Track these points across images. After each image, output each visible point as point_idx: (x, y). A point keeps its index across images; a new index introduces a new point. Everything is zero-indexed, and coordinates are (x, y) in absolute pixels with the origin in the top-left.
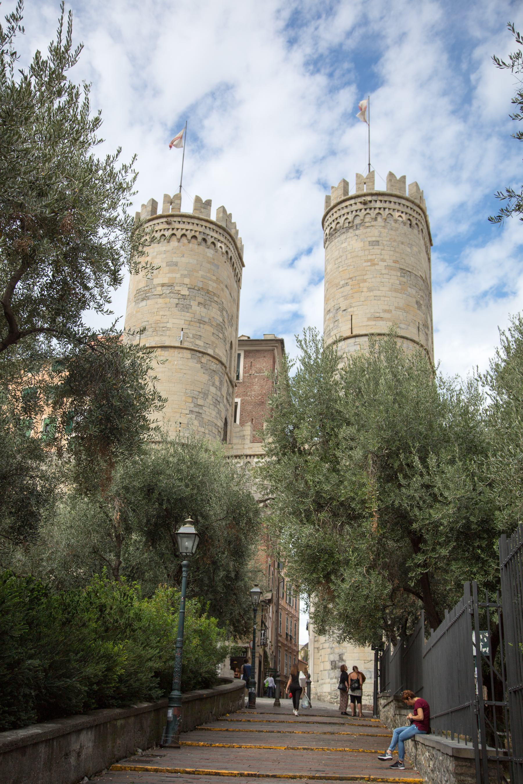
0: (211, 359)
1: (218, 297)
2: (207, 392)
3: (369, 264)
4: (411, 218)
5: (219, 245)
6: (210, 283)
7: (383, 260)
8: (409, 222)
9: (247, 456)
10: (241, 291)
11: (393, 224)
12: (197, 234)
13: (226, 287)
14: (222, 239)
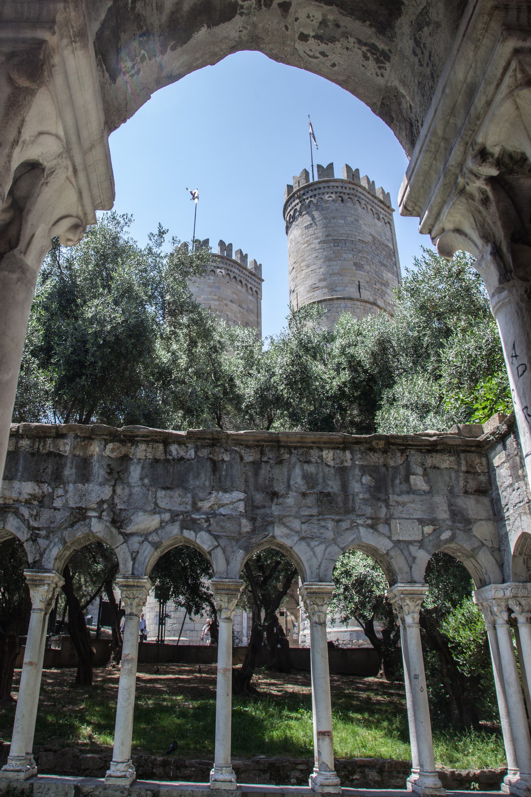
3: (306, 245)
4: (342, 195)
5: (218, 270)
6: (212, 302)
7: (317, 238)
8: (340, 199)
11: (324, 205)
13: (231, 301)
14: (221, 265)
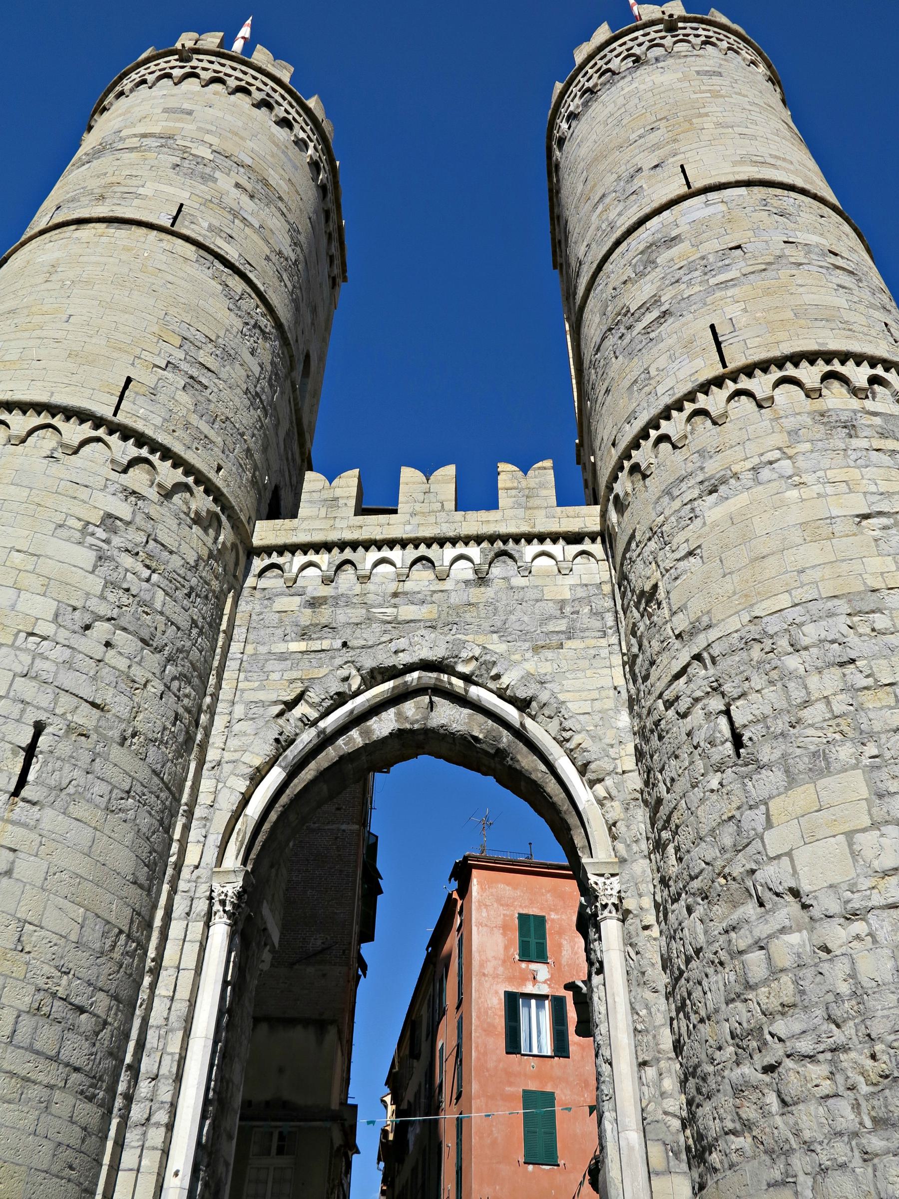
0: (253, 295)
1: (289, 210)
2: (232, 352)
9: (342, 545)
10: (337, 315)
12: (253, 89)
